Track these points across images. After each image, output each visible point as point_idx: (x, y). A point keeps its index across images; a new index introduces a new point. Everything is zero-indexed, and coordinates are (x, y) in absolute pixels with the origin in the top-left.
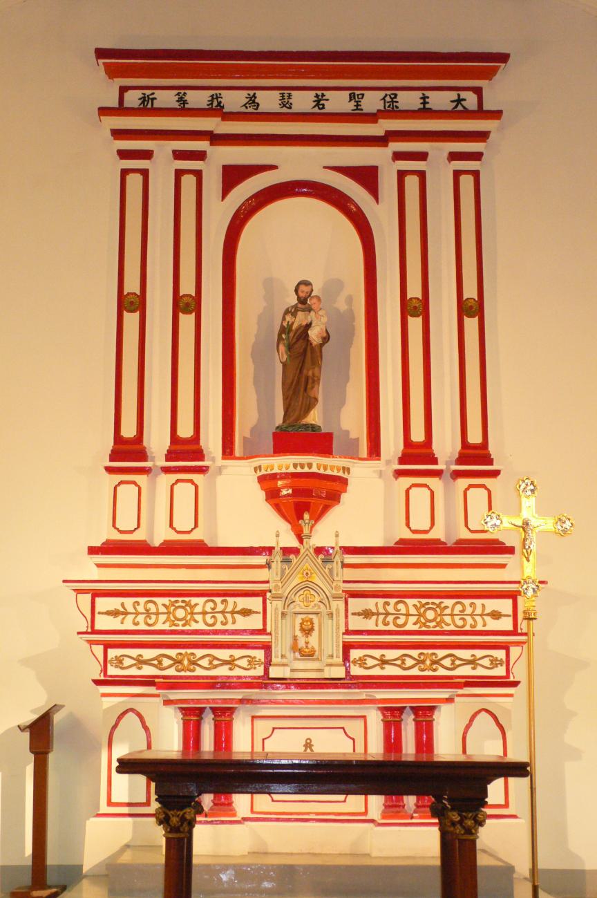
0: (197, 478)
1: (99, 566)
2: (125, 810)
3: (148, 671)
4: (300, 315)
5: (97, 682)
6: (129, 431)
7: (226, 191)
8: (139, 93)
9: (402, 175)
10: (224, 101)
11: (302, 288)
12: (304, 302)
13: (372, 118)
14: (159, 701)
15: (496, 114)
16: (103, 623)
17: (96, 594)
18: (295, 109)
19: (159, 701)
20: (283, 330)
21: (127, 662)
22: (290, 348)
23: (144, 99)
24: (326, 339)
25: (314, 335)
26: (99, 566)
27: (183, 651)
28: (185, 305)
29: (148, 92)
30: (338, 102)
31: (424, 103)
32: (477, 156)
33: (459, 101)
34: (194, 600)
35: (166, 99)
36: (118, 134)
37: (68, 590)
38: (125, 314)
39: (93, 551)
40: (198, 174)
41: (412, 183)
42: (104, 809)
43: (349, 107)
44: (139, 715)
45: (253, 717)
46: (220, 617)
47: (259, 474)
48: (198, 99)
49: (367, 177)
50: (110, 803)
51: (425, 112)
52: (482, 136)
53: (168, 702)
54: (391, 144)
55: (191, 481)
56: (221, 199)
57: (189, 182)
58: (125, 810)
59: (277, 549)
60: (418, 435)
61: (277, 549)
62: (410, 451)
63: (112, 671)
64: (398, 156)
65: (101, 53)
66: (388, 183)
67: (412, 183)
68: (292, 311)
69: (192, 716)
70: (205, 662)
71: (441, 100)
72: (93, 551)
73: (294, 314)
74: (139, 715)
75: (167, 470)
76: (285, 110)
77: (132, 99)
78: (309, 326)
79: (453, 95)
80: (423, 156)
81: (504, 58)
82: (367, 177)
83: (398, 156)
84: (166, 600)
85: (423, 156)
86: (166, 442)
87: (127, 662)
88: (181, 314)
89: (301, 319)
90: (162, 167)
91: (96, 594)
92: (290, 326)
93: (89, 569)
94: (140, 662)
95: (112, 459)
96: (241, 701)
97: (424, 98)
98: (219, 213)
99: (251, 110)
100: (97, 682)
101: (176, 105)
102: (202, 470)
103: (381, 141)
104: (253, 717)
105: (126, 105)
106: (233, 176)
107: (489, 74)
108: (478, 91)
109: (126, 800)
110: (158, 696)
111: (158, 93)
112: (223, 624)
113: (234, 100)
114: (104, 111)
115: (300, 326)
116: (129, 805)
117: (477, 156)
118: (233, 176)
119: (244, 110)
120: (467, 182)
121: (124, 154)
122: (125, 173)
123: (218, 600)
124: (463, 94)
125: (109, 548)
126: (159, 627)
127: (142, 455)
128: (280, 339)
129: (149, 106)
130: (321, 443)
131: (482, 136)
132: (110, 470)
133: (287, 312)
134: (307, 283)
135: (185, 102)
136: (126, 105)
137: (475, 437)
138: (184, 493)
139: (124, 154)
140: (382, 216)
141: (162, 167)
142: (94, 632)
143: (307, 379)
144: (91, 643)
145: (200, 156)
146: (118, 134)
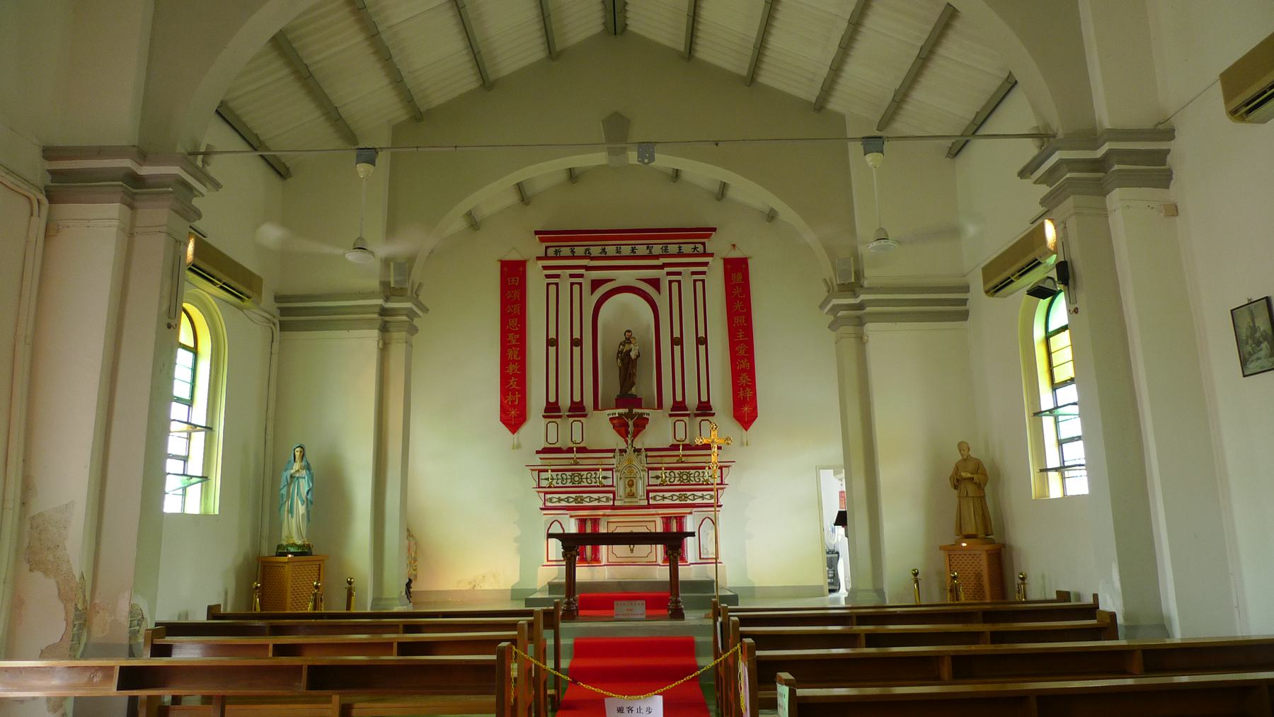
0: (582, 419)
1: (541, 459)
2: (555, 563)
3: (563, 504)
4: (627, 346)
5: (542, 509)
6: (552, 399)
7: (593, 291)
8: (554, 249)
9: (670, 282)
10: (591, 251)
11: (627, 333)
12: (628, 340)
13: (657, 257)
14: (568, 516)
15: (711, 255)
16: (544, 483)
17: (540, 471)
18: (622, 254)
19: (568, 516)
20: (619, 352)
21: (658, 498)
22: (622, 360)
23: (556, 252)
24: (638, 356)
25: (633, 355)
26: (541, 459)
27: (578, 495)
28: (576, 343)
29: (558, 248)
30: (642, 250)
31: (680, 250)
32: (704, 273)
33: (695, 248)
34: (582, 473)
35: (566, 251)
36: (545, 268)
37: (528, 470)
38: (700, 346)
39: (538, 452)
40: (580, 284)
41: (675, 285)
42: (546, 563)
43: (646, 252)
44: (559, 522)
45: (608, 522)
46: (593, 480)
47: (610, 417)
48: (580, 251)
49: (655, 283)
50: (548, 561)
51: (680, 255)
52: (706, 264)
53: (571, 517)
54: (665, 269)
55: (580, 421)
56: (590, 293)
57: (576, 288)
58: (555, 563)
59: (643, 449)
60: (679, 398)
61: (643, 449)
62: (701, 405)
63: (549, 504)
64: (669, 274)
65: (537, 233)
66: (664, 285)
67: (675, 285)
68: (623, 344)
69: (582, 522)
70: (588, 500)
71: (687, 249)
72: (538, 452)
73: (624, 345)
74: (559, 522)
75: (569, 416)
76: (618, 255)
77: (551, 252)
78: (630, 350)
79: (693, 246)
80: (679, 274)
81: (714, 230)
82: (655, 283)
83: (669, 274)
84: (570, 473)
85: (679, 274)
86: (671, 403)
87: (658, 498)
88: (700, 346)
89: (627, 347)
90: (565, 284)
91: (540, 471)
92: (622, 350)
93: (537, 460)
94: (560, 500)
95: (545, 412)
96: (604, 515)
97: (680, 247)
98: (591, 300)
99: (603, 255)
100: (542, 509)
101: (571, 254)
102: (585, 416)
103: (661, 267)
104: (608, 522)
105: (548, 255)
106: (596, 284)
107: (708, 236)
108: (704, 244)
109: (555, 559)
110: (567, 514)
111: (562, 249)
112: (595, 483)
113: (596, 251)
114: (539, 258)
115: (626, 351)
116: (556, 561)
117: (704, 273)
118: (596, 284)
119: (600, 255)
120: (699, 284)
121: (548, 276)
122: (548, 284)
123: (593, 472)
124: (697, 245)
125: (545, 451)
126: (567, 485)
127: (558, 410)
128: (618, 356)
129: (558, 255)
130: (637, 402)
131: (706, 264)
132: (544, 417)
133: (621, 344)
134: (629, 331)
135: (574, 252)
136: (548, 255)
137: (704, 399)
138: (577, 426)
139: (548, 276)
140: (662, 301)
141: (565, 284)
142: (539, 487)
143: (630, 374)
144: (539, 492)
145: (581, 276)
146: (545, 268)
